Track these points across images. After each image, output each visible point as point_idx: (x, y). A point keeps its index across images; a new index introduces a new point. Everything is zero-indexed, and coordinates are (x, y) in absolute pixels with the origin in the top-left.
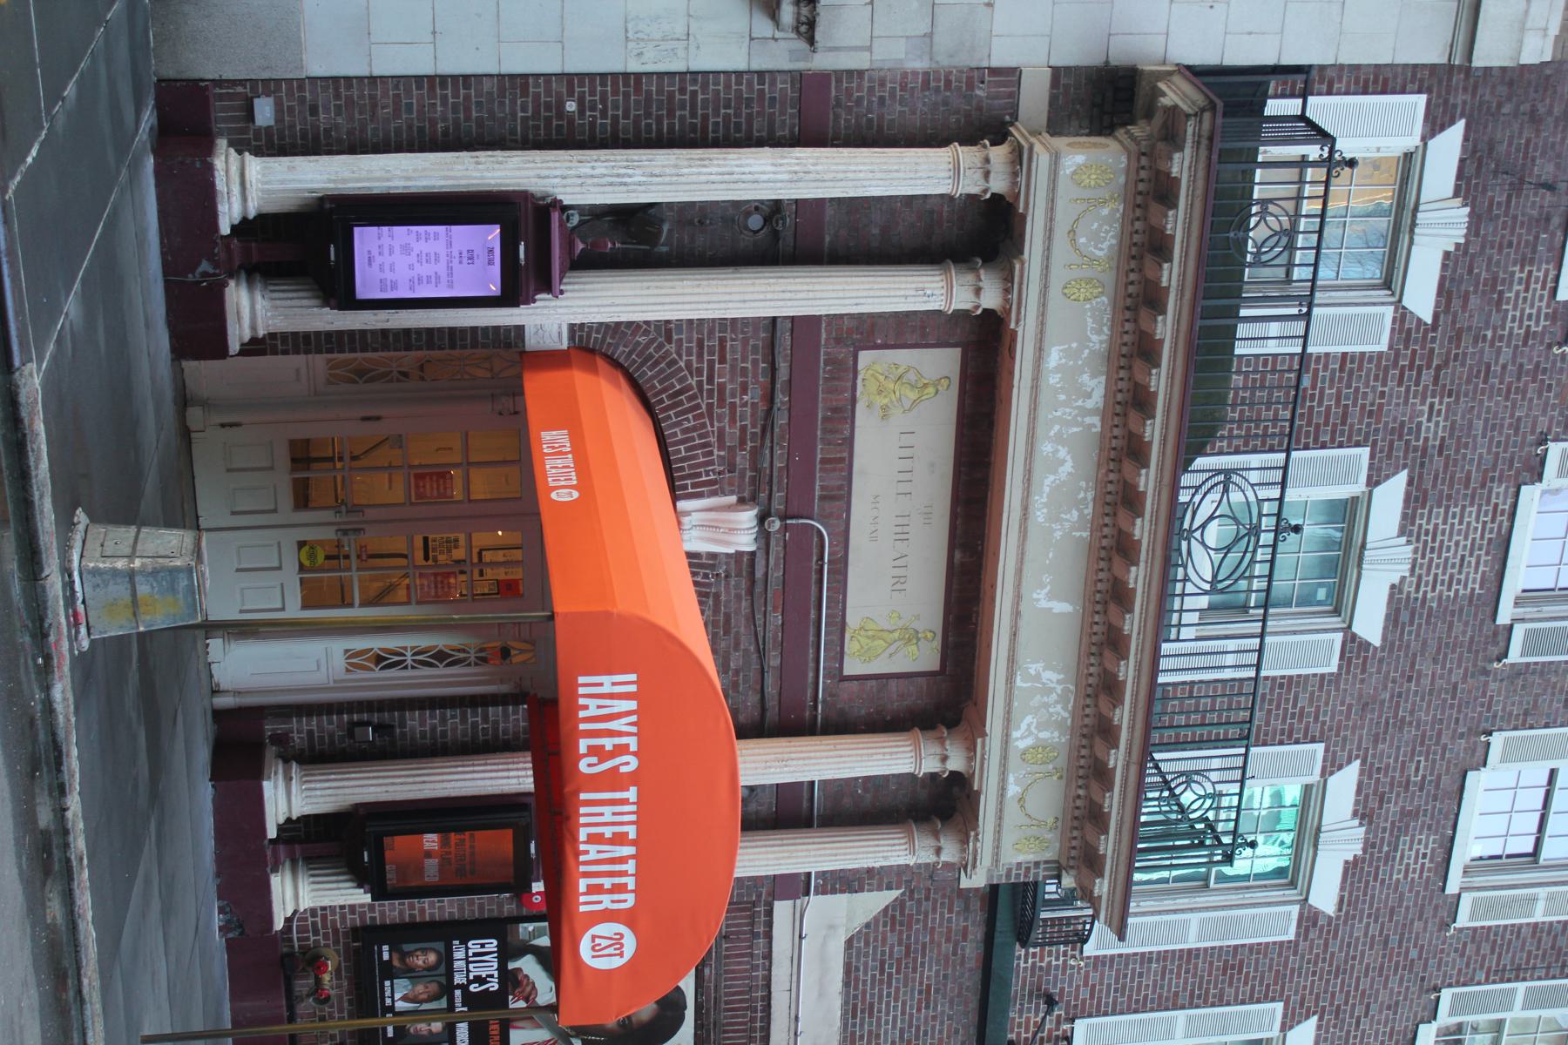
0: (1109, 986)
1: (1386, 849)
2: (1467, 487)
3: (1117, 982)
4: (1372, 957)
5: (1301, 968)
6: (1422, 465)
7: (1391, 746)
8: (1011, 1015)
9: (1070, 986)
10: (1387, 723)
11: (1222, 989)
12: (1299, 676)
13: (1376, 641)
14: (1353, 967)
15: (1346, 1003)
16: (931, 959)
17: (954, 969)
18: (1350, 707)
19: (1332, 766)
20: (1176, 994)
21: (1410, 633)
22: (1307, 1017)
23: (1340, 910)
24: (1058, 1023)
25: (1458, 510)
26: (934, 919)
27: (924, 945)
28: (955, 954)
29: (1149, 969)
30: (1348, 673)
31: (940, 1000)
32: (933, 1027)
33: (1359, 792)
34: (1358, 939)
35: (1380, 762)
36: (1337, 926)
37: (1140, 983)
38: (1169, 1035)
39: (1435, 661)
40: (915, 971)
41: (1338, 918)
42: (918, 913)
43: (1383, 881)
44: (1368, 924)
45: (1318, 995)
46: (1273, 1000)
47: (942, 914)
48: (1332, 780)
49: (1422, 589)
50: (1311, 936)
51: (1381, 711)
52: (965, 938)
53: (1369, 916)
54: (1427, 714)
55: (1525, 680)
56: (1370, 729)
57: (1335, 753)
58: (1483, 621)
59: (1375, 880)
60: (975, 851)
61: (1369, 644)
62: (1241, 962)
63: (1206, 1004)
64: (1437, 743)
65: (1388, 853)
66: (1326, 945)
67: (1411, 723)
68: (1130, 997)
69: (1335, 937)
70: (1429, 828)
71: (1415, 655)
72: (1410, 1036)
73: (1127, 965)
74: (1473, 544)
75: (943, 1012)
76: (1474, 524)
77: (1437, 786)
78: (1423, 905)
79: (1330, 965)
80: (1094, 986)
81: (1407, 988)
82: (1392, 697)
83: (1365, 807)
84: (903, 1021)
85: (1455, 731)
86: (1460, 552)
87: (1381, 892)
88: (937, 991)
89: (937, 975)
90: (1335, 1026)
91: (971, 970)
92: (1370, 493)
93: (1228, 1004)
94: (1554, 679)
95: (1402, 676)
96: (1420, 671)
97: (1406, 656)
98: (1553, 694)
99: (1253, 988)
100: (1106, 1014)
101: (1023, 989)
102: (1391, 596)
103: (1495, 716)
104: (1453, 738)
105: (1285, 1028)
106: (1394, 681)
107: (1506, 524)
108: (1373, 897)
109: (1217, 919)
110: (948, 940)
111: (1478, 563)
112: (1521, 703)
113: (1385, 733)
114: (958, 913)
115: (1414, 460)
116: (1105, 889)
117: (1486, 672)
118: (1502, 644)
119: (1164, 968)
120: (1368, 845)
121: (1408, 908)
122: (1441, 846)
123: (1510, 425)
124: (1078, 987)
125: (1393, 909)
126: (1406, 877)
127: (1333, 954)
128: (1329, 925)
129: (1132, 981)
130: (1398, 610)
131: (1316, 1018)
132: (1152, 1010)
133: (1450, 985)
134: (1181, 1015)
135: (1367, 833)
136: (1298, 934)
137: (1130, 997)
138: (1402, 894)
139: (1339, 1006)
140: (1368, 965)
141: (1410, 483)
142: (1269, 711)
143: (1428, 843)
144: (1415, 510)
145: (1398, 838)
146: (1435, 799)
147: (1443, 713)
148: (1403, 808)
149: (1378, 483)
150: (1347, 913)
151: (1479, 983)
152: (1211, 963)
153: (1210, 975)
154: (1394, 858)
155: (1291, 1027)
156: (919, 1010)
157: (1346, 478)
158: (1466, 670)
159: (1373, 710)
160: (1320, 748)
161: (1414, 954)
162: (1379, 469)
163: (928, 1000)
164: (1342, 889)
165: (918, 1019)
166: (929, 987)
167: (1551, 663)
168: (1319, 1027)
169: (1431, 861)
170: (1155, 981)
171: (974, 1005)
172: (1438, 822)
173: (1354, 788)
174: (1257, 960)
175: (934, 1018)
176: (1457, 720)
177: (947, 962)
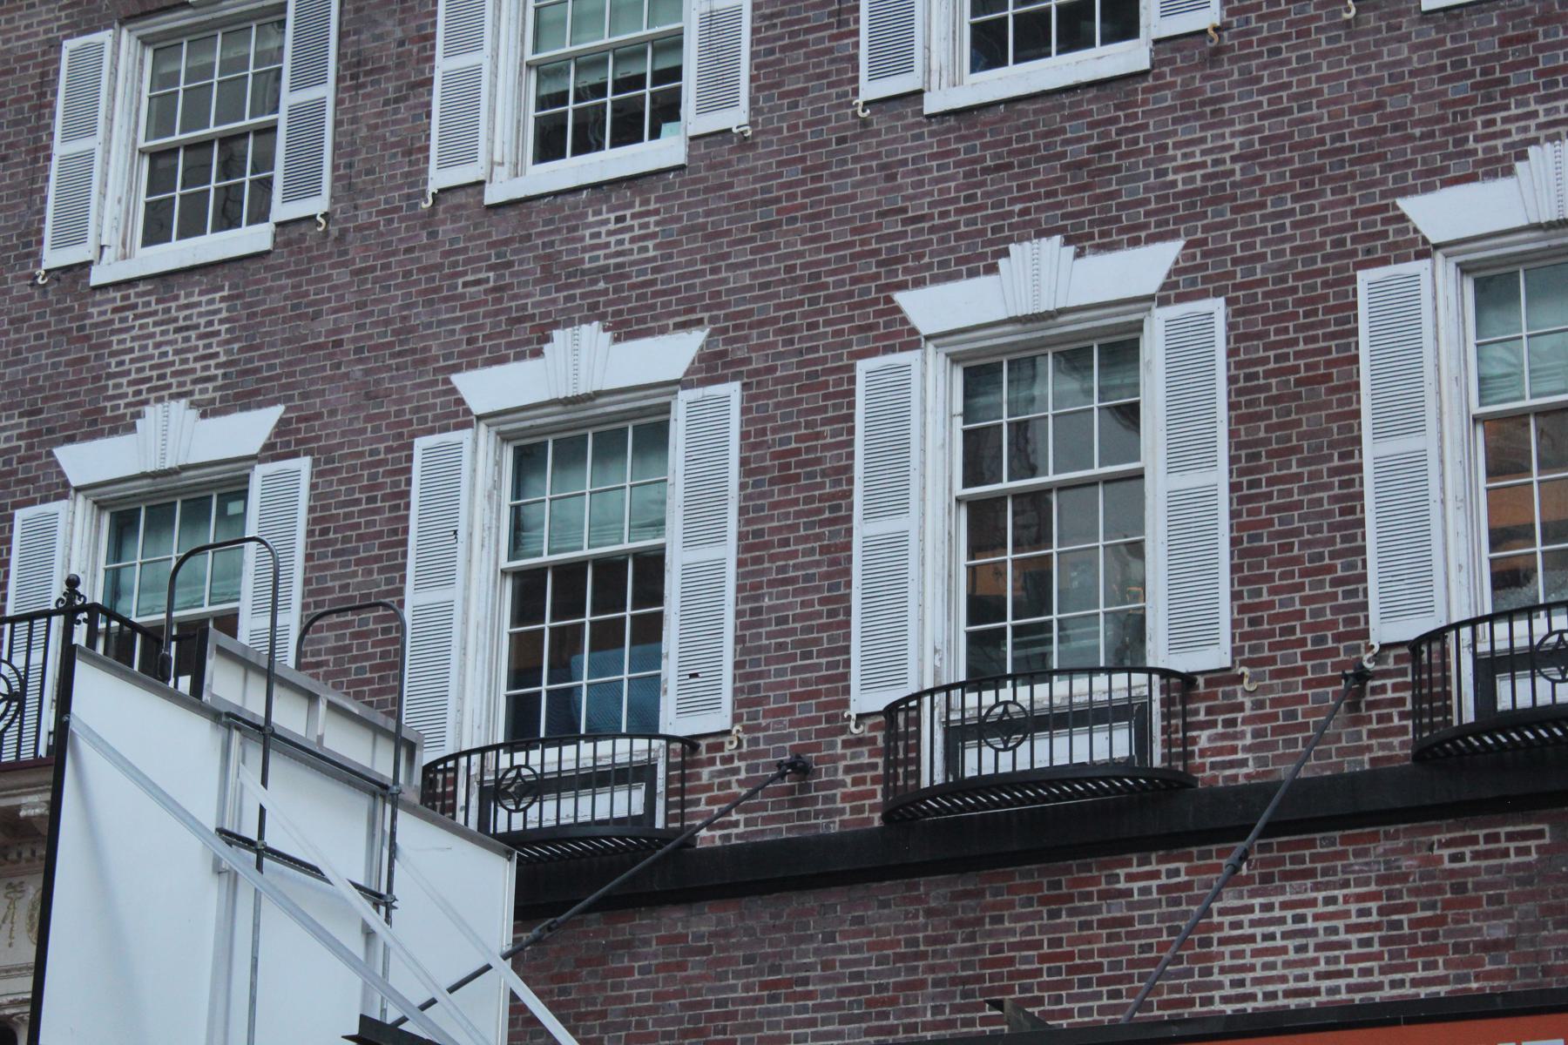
0: (795, 670)
1: (602, 285)
2: (85, 360)
3: (792, 658)
4: (791, 242)
5: (800, 352)
6: (50, 431)
7: (435, 336)
8: (835, 829)
9: (790, 737)
10: (400, 354)
11: (824, 474)
12: (311, 510)
13: (277, 412)
14: (804, 266)
15: (877, 252)
16: (711, 990)
17: (738, 946)
18: (369, 419)
19: (458, 416)
20: (825, 550)
21: (271, 367)
22: (898, 310)
23: (700, 322)
24: (859, 742)
25: (113, 361)
26: (640, 997)
27: (686, 1006)
28: (707, 951)
29: (771, 609)
30: (318, 438)
31: (796, 960)
32: (845, 964)
33: (502, 360)
34: (754, 276)
35: (457, 343)
36: (727, 317)
37: (796, 618)
38: (898, 542)
39: (317, 315)
40: (732, 1016)
41: (713, 320)
42: (626, 1026)
43: (655, 270)
44: (731, 267)
45: (852, 307)
46: (852, 380)
47: (633, 985)
48: (478, 404)
49: (213, 372)
50: (740, 355)
51: (379, 370)
52: (682, 938)
53: (714, 271)
54: (394, 298)
55: (359, 175)
56: (406, 377)
57: (436, 418)
58: (267, 269)
59: (652, 283)
60: (13, 1004)
61: (282, 422)
62: (775, 456)
63: (849, 494)
64: (439, 267)
65: (607, 279)
66: (761, 323)
67: (404, 318)
68: (822, 628)
69: (750, 313)
70: (575, 228)
71: (305, 349)
72: (952, 121)
73: (760, 649)
74: (162, 323)
75: (817, 952)
76: (135, 332)
77: (506, 242)
78: (707, 190)
79: (800, 303)
80: (794, 697)
81: (856, 160)
82: (360, 361)
83: (528, 342)
84: (825, 1021)
85: (424, 248)
86: (171, 337)
87: (676, 266)
88: (775, 969)
89: (747, 974)
90: (922, 256)
91: (742, 917)
92: (78, 490)
93: (851, 456)
94: (364, 132)
95: (330, 356)
96: (330, 333)
97: (302, 361)
98: (385, 124)
99: (826, 422)
100: (847, 663)
101: (786, 818)
102: (216, 413)
103: (409, 197)
104: (432, 247)
105: (910, 339)
106: (338, 366)
107: (141, 288)
108: (681, 277)
109: (687, 519)
110: (681, 966)
111: (187, 307)
112: (392, 167)
113: (413, 351)
114: (634, 957)
115: (41, 444)
116: (34, 799)
117: (341, 238)
118: (304, 228)
119: (771, 584)
120: (592, 313)
121: (708, 214)
122: (607, 199)
123: (17, 331)
124: (793, 724)
125: (707, 237)
126: (654, 235)
127: (778, 307)
128: (725, 330)
129: (793, 632)
130: (237, 396)
131: (900, 297)
132: (849, 584)
133: (856, 92)
134: (862, 529)
135: (570, 323)
136: (735, 377)
137: (822, 628)
138: (683, 231)
139: (879, 264)
140: (805, 242)
141: (71, 439)
142: (360, 538)
143: (601, 223)
144: (107, 420)
145: (584, 272)
146: (528, 237)
147: (395, 276)
148: (536, 282)
149: (66, 484)
150: (707, 308)
151: (857, 45)
152: (774, 506)
153: (795, 502)
154: (618, 266)
155: (914, 331)
156: (809, 995)
157: (46, 530)
158: (333, 266)
159: (378, 382)
160: (421, 443)
161: (791, 174)
162: (49, 487)
163: (788, 983)
164: (663, 331)
165: (826, 994)
166: (764, 986)
167: (337, 146)
168: (919, 283)
169: (631, 205)
170: (796, 593)
171: (810, 900)
172: (567, 219)
173: (496, 369)
174: (775, 431)
175: (827, 965)
176: (407, 251)
177: (718, 962)
